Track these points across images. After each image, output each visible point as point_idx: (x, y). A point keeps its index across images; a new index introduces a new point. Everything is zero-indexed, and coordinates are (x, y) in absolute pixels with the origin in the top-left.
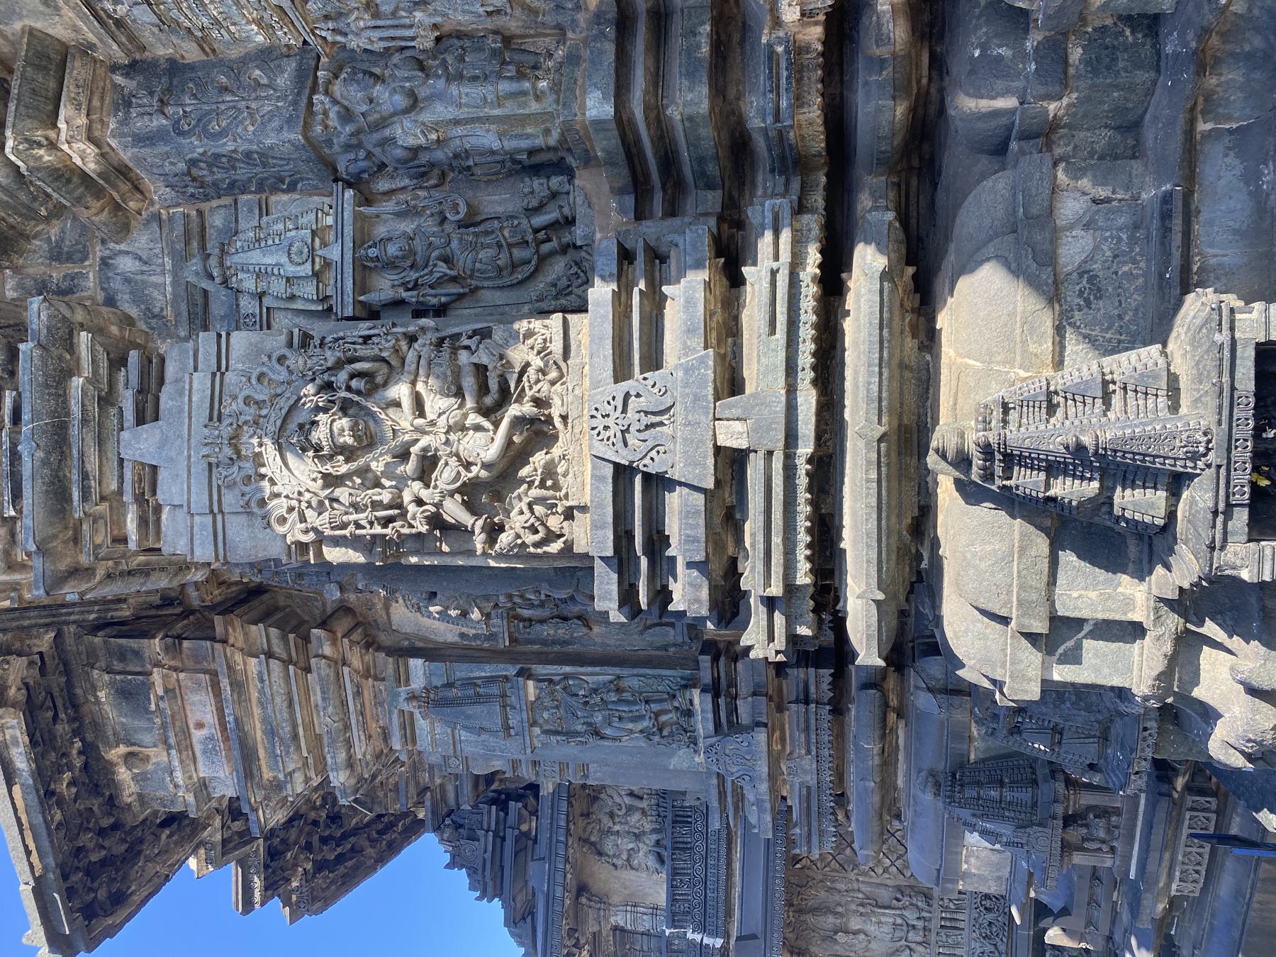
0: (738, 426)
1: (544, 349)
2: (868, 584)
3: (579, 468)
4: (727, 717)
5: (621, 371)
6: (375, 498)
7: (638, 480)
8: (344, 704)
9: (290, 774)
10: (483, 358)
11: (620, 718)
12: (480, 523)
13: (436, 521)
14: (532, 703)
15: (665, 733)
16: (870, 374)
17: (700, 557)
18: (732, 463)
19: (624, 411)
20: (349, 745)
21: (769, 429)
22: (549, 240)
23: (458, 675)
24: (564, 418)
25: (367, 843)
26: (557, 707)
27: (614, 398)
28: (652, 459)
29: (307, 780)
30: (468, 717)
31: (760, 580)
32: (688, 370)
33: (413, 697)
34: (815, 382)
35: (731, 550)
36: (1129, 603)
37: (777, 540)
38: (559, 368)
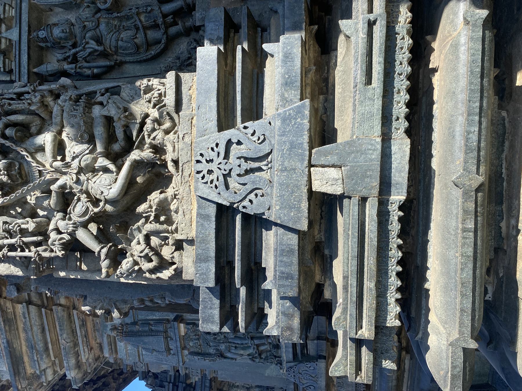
0: (333, 173)
1: (160, 101)
2: (461, 333)
3: (189, 204)
4: (301, 351)
5: (225, 122)
6: (23, 226)
7: (238, 218)
8: (73, 332)
9: (44, 370)
10: (112, 111)
11: (236, 347)
12: (105, 250)
13: (73, 246)
14: (183, 336)
15: (263, 356)
16: (470, 123)
17: (293, 293)
18: (325, 206)
19: (227, 156)
20: (77, 355)
21: (364, 176)
22: (175, 24)
23: (140, 317)
24: (176, 162)
25: (112, 380)
26: (198, 339)
27: (217, 145)
28: (251, 201)
29: (55, 372)
30: (145, 343)
31: (350, 321)
32: (285, 119)
33: (114, 328)
34: (408, 132)
35: (318, 278)
37: (369, 284)
38: (172, 118)
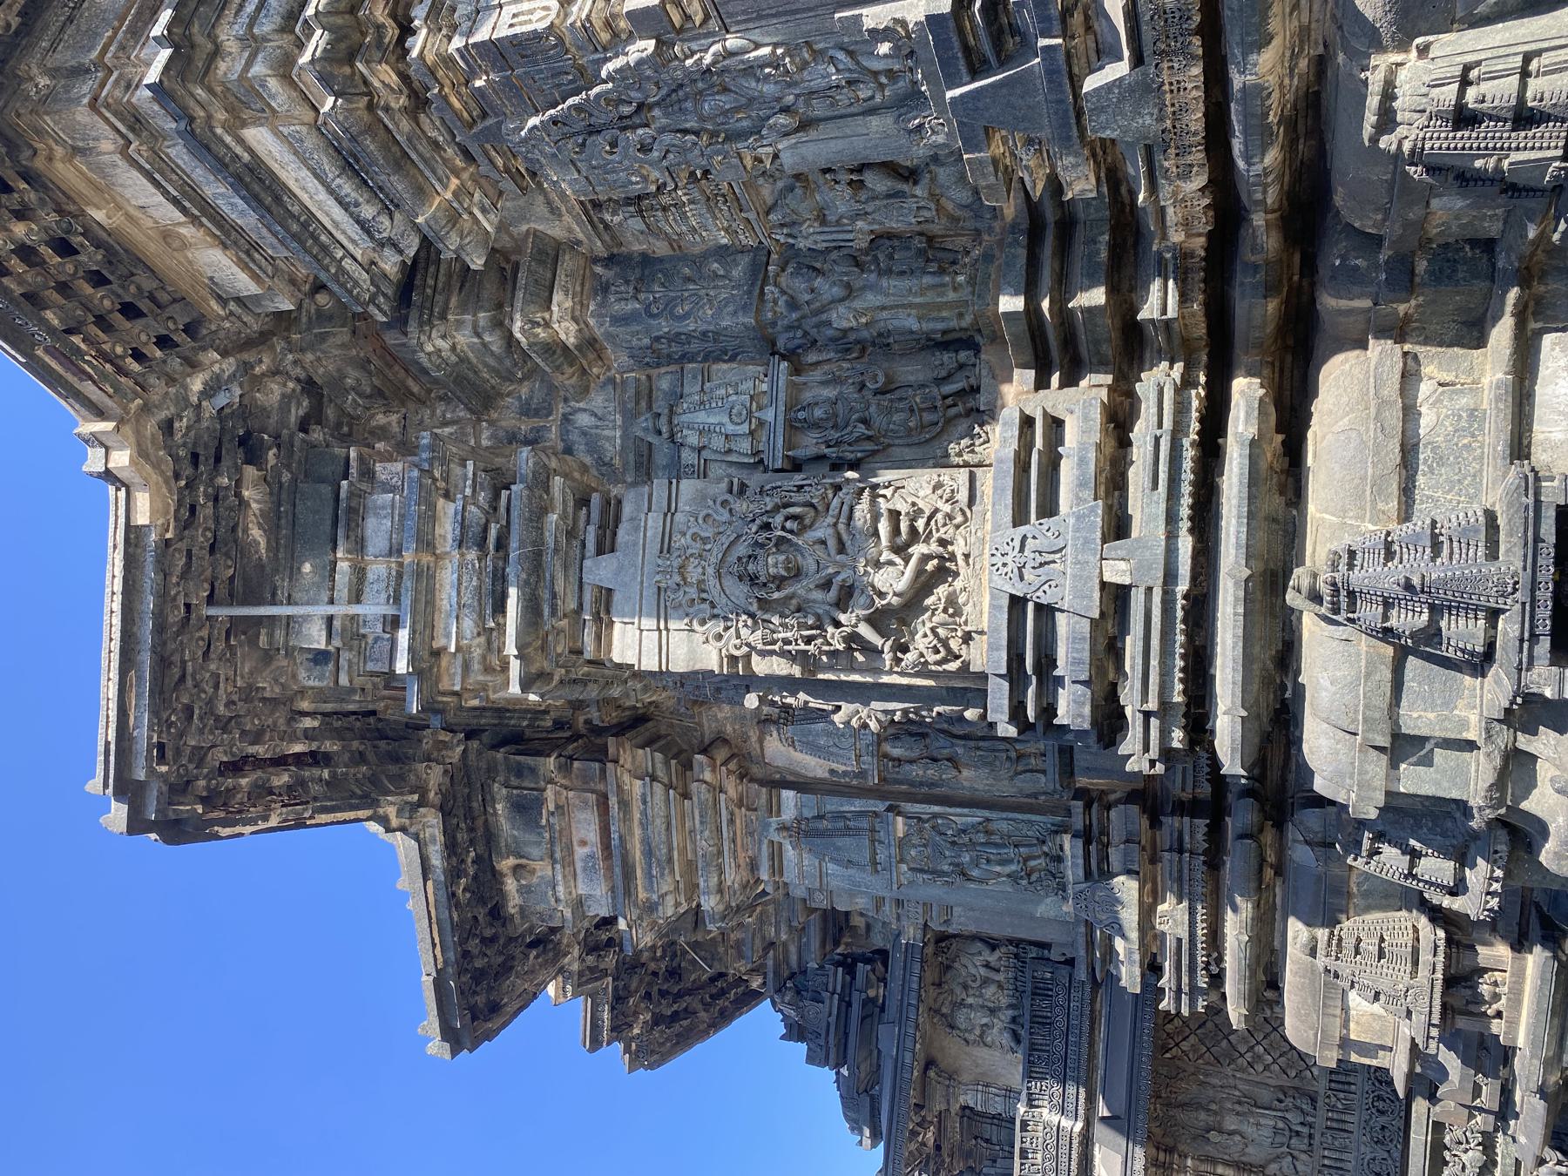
0: (1123, 565)
1: (952, 498)
2: (1233, 702)
3: (980, 596)
4: (1099, 868)
5: (1020, 518)
7: (1030, 606)
8: (719, 830)
9: (663, 896)
11: (988, 861)
12: (890, 643)
13: (853, 639)
14: (901, 840)
15: (1034, 877)
16: (1239, 524)
17: (1084, 677)
18: (1116, 597)
19: (1022, 550)
20: (721, 872)
21: (1150, 568)
22: (955, 405)
23: (829, 808)
24: (967, 556)
25: (700, 1006)
26: (925, 846)
29: (677, 904)
30: (838, 849)
31: (1137, 696)
32: (1079, 518)
33: (783, 828)
34: (1191, 531)
35: (1111, 676)
36: (1464, 724)
37: (1154, 662)
38: (964, 513)
